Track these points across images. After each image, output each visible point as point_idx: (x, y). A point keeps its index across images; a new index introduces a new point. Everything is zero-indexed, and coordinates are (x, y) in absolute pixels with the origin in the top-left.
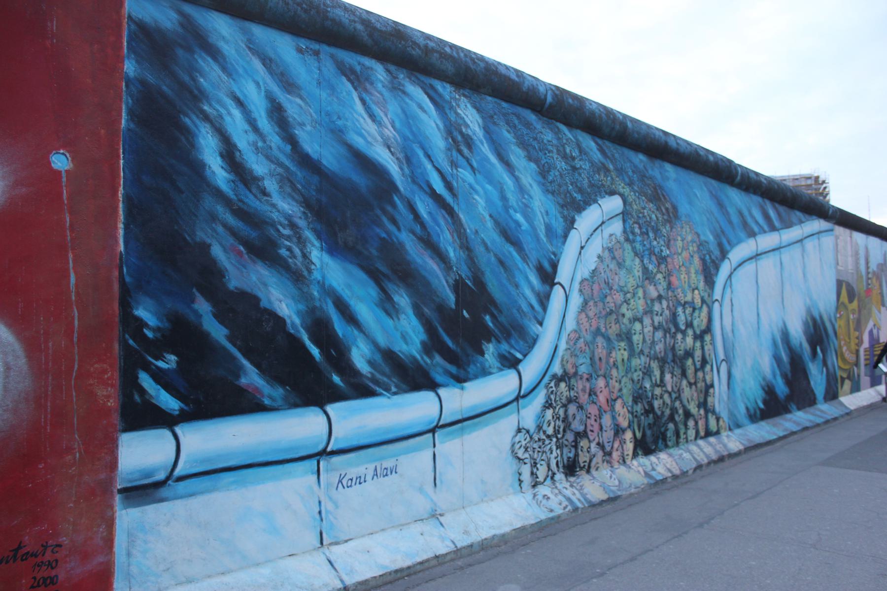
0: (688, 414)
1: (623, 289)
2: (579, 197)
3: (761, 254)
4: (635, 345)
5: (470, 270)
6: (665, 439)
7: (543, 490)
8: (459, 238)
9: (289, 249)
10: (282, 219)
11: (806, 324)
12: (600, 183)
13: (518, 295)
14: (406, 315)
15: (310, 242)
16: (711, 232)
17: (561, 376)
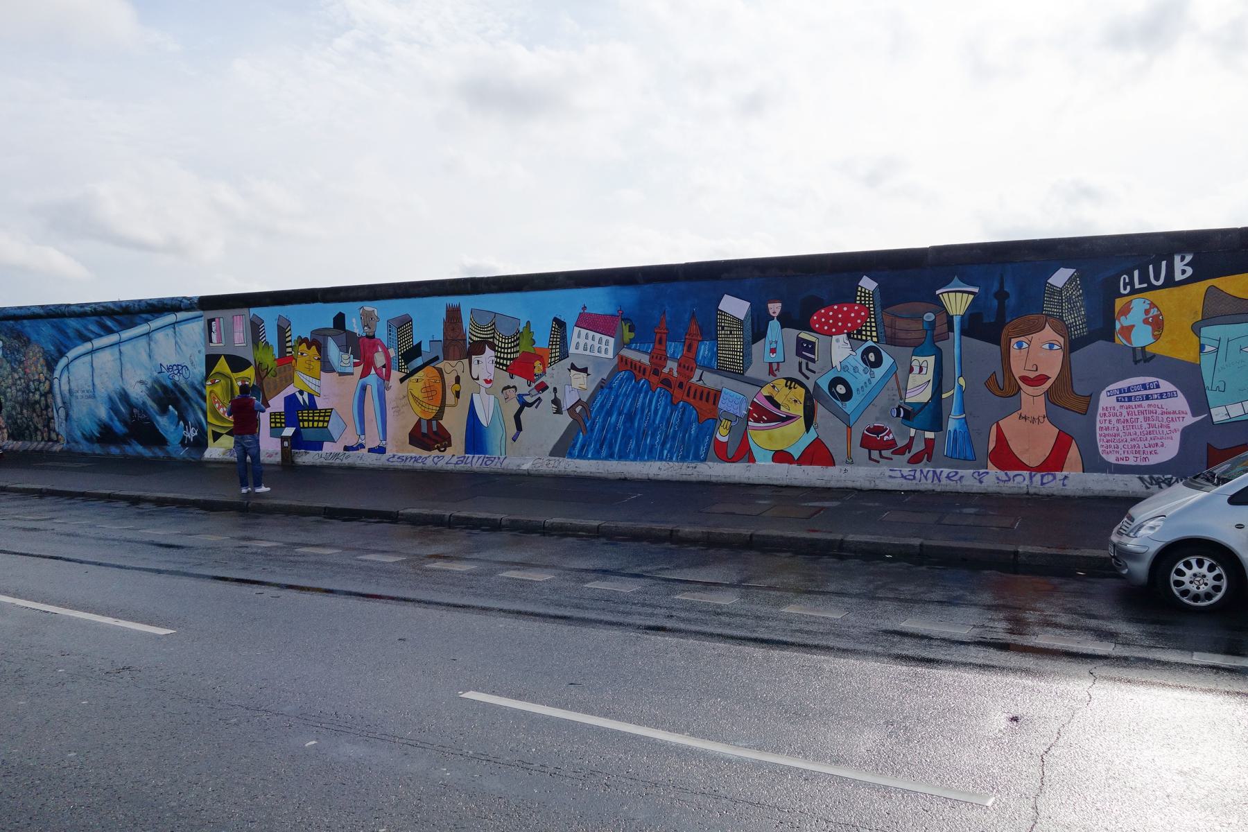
0: (36, 429)
16: (53, 346)
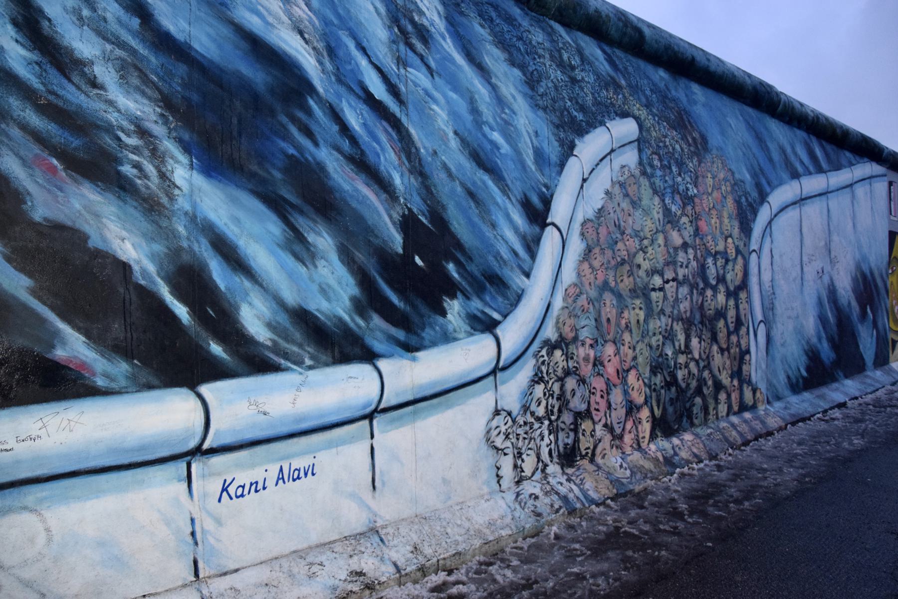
0: (718, 386)
1: (638, 233)
2: (580, 116)
3: (806, 199)
4: (654, 304)
5: (425, 202)
6: (690, 417)
7: (529, 488)
8: (409, 158)
9: (137, 166)
10: (125, 123)
11: (855, 280)
12: (609, 101)
13: (495, 237)
14: (327, 261)
15: (172, 157)
16: (748, 170)
17: (556, 341)
